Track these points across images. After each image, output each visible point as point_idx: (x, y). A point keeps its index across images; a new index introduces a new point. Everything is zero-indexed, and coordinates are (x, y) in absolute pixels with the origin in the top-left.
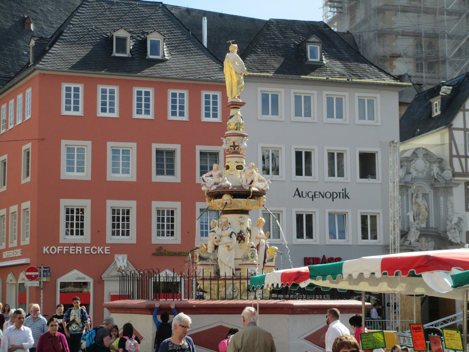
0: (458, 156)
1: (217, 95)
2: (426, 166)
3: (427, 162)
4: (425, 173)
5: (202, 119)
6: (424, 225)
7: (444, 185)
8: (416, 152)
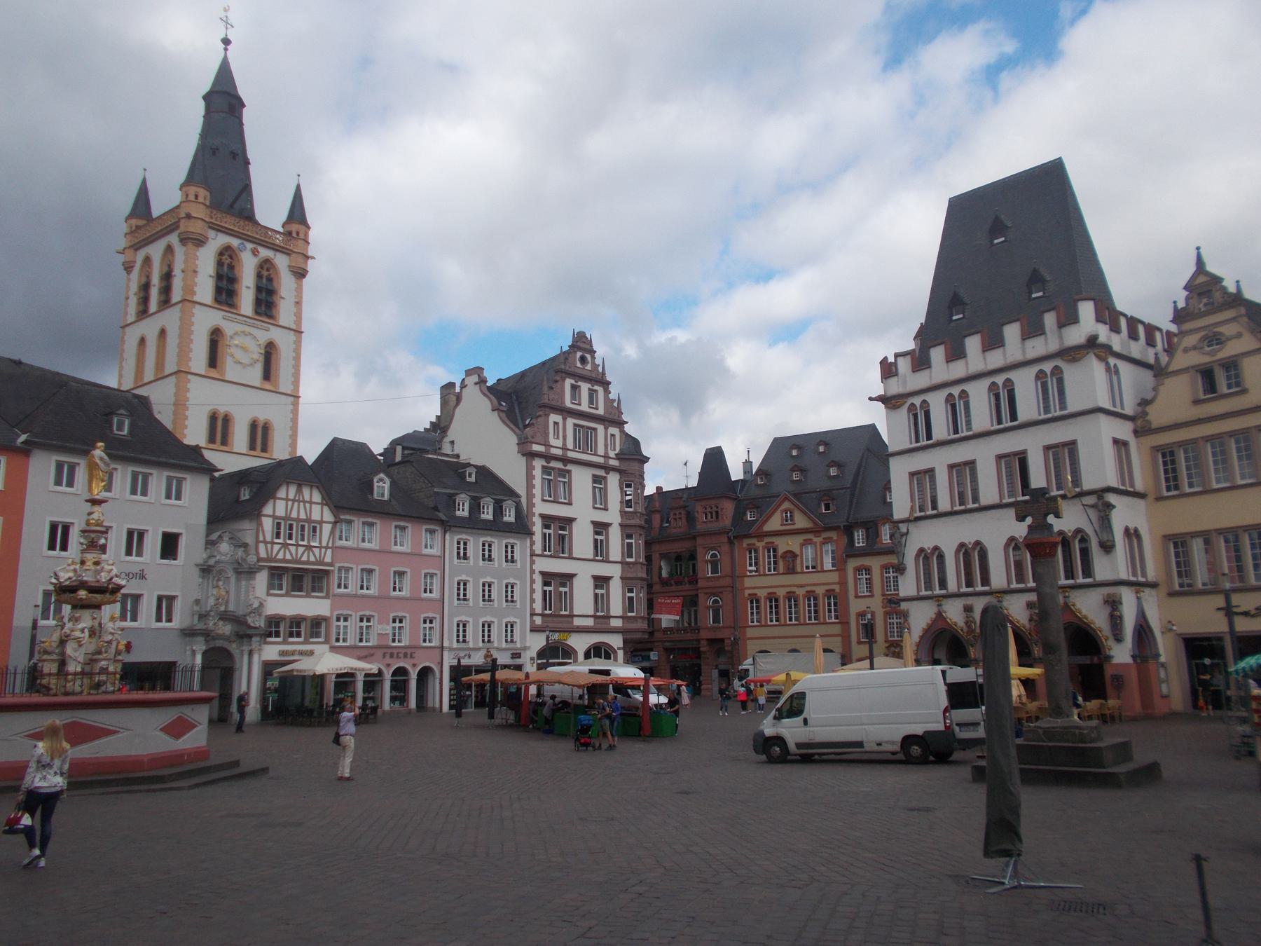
0: (265, 542)
4: (229, 556)
6: (222, 608)
7: (247, 570)
8: (222, 535)
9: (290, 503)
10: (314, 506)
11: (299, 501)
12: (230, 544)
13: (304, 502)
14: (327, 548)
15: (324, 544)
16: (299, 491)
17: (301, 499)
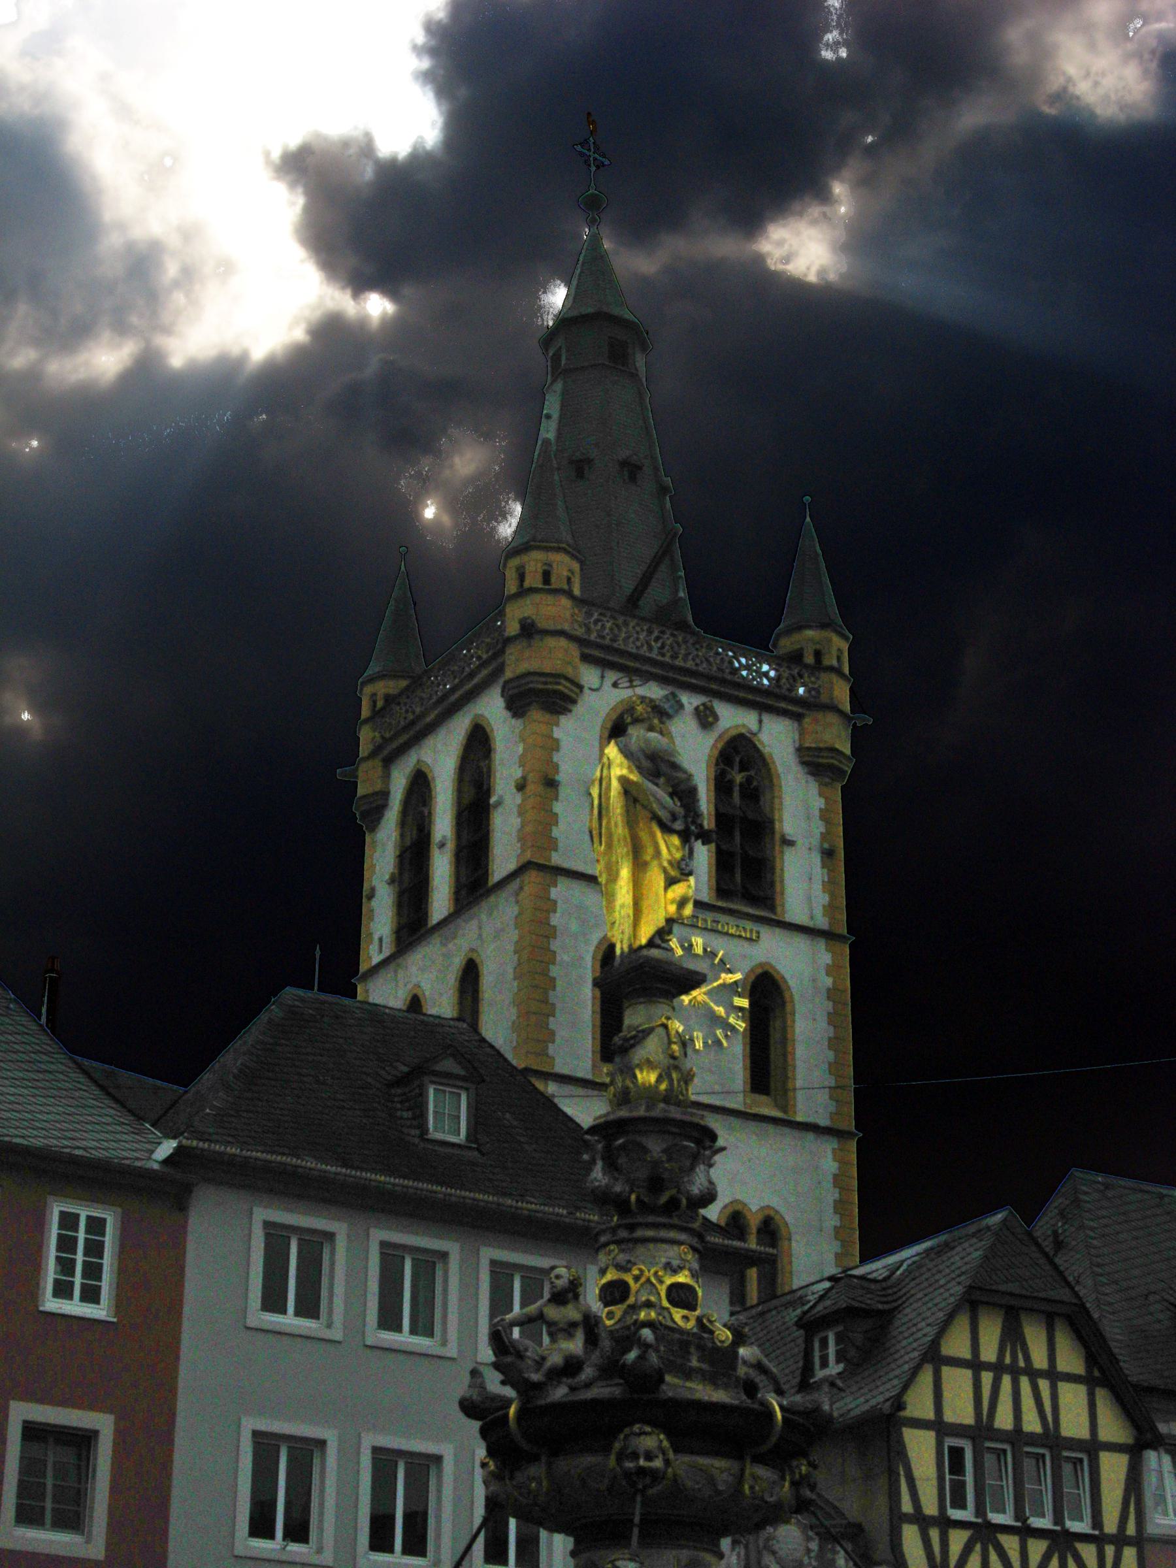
1: (105, 1220)
2: (809, 1551)
3: (810, 1533)
5: (40, 1303)
9: (987, 1378)
11: (1015, 1373)
12: (804, 1532)
13: (1034, 1375)
14: (1120, 1540)
15: (1110, 1526)
17: (1022, 1364)
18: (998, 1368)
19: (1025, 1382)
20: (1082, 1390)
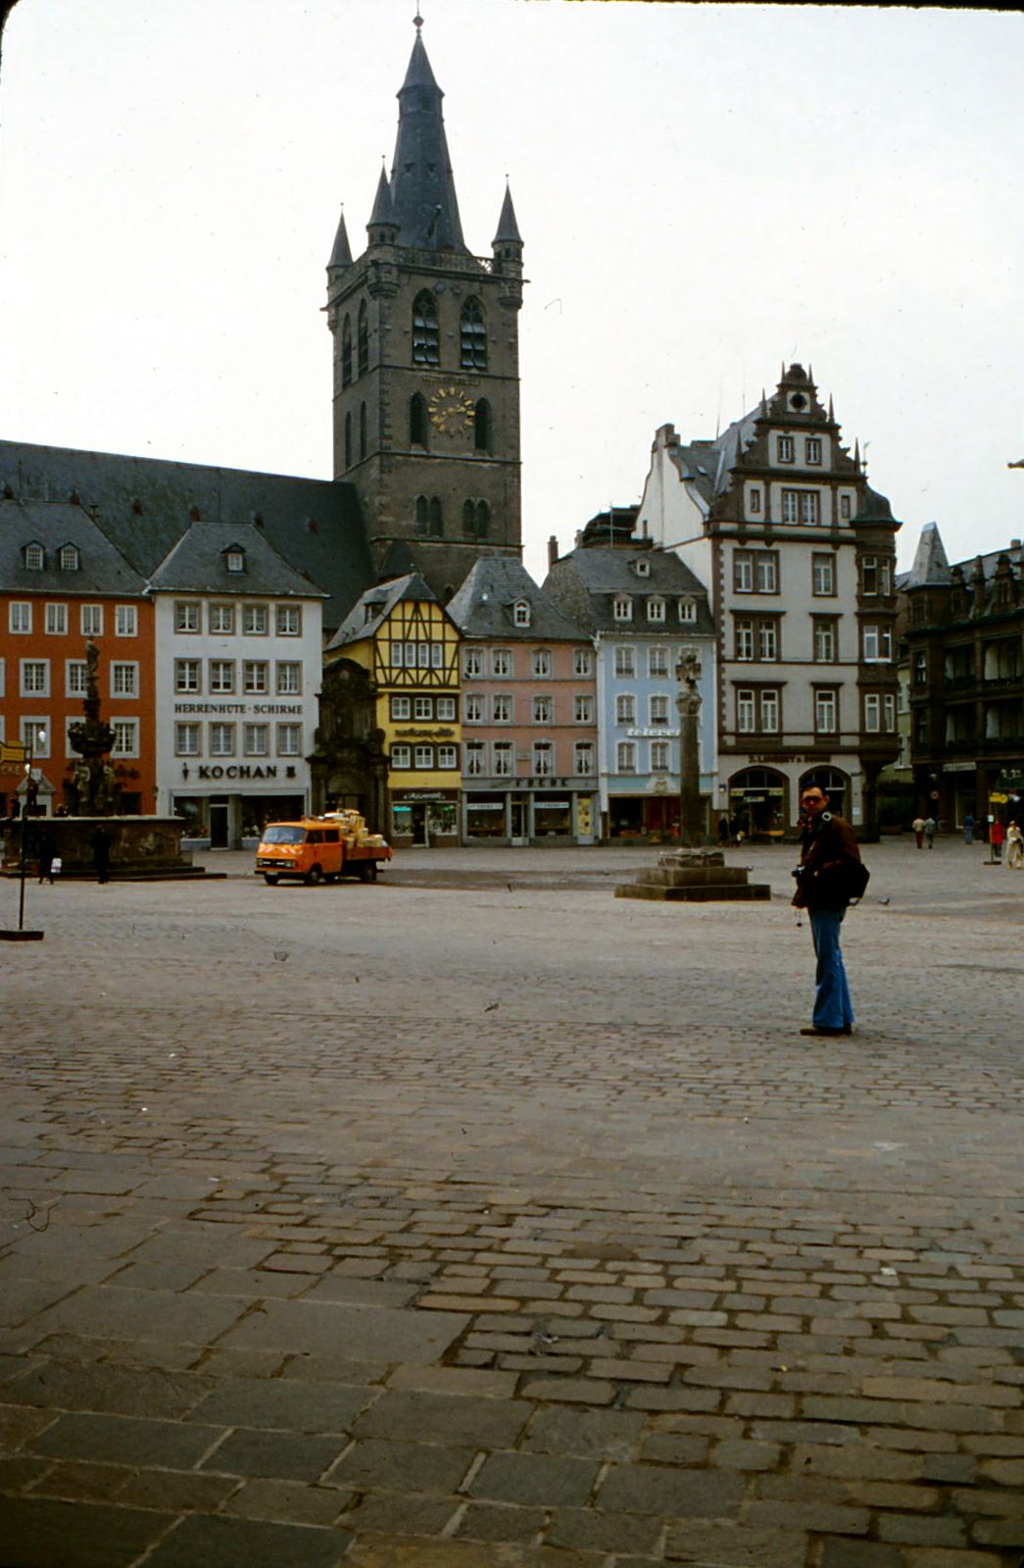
0: (383, 667)
9: (407, 624)
10: (434, 625)
11: (417, 622)
13: (423, 622)
16: (417, 610)
18: (411, 621)
19: (420, 625)
20: (441, 625)
